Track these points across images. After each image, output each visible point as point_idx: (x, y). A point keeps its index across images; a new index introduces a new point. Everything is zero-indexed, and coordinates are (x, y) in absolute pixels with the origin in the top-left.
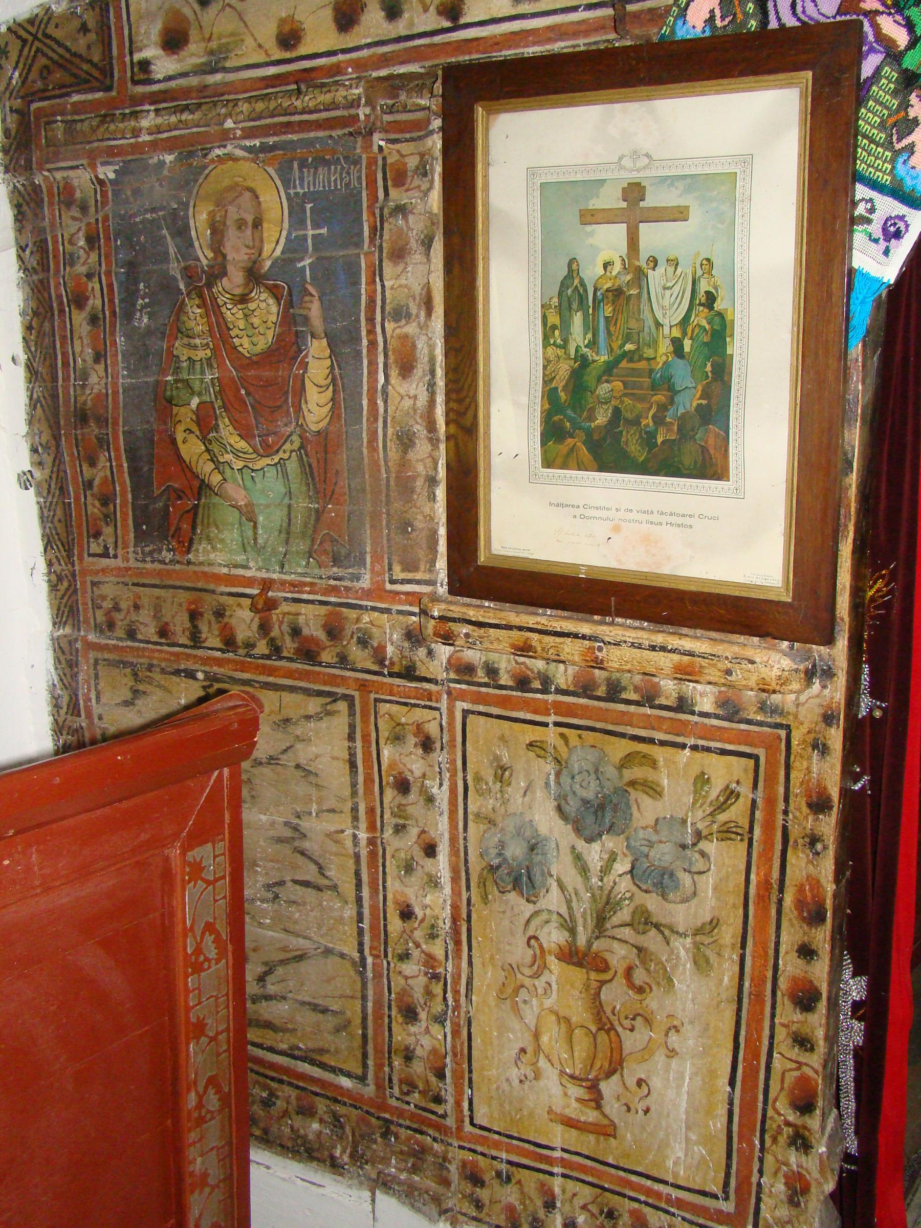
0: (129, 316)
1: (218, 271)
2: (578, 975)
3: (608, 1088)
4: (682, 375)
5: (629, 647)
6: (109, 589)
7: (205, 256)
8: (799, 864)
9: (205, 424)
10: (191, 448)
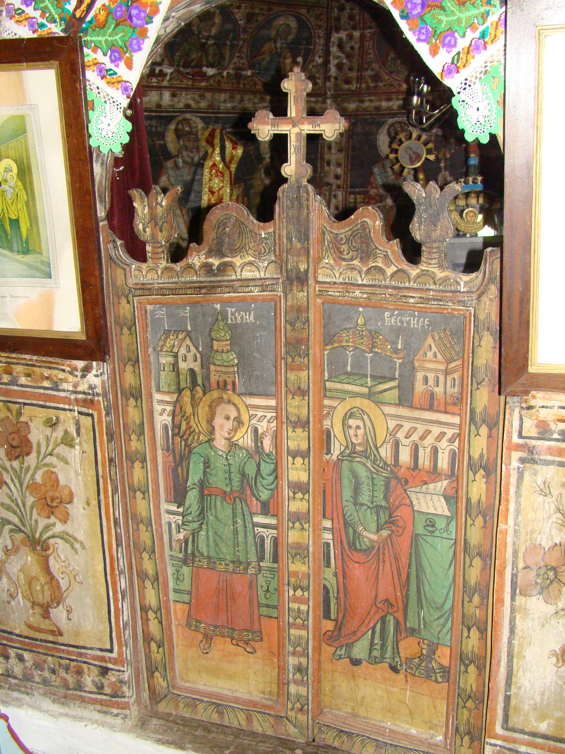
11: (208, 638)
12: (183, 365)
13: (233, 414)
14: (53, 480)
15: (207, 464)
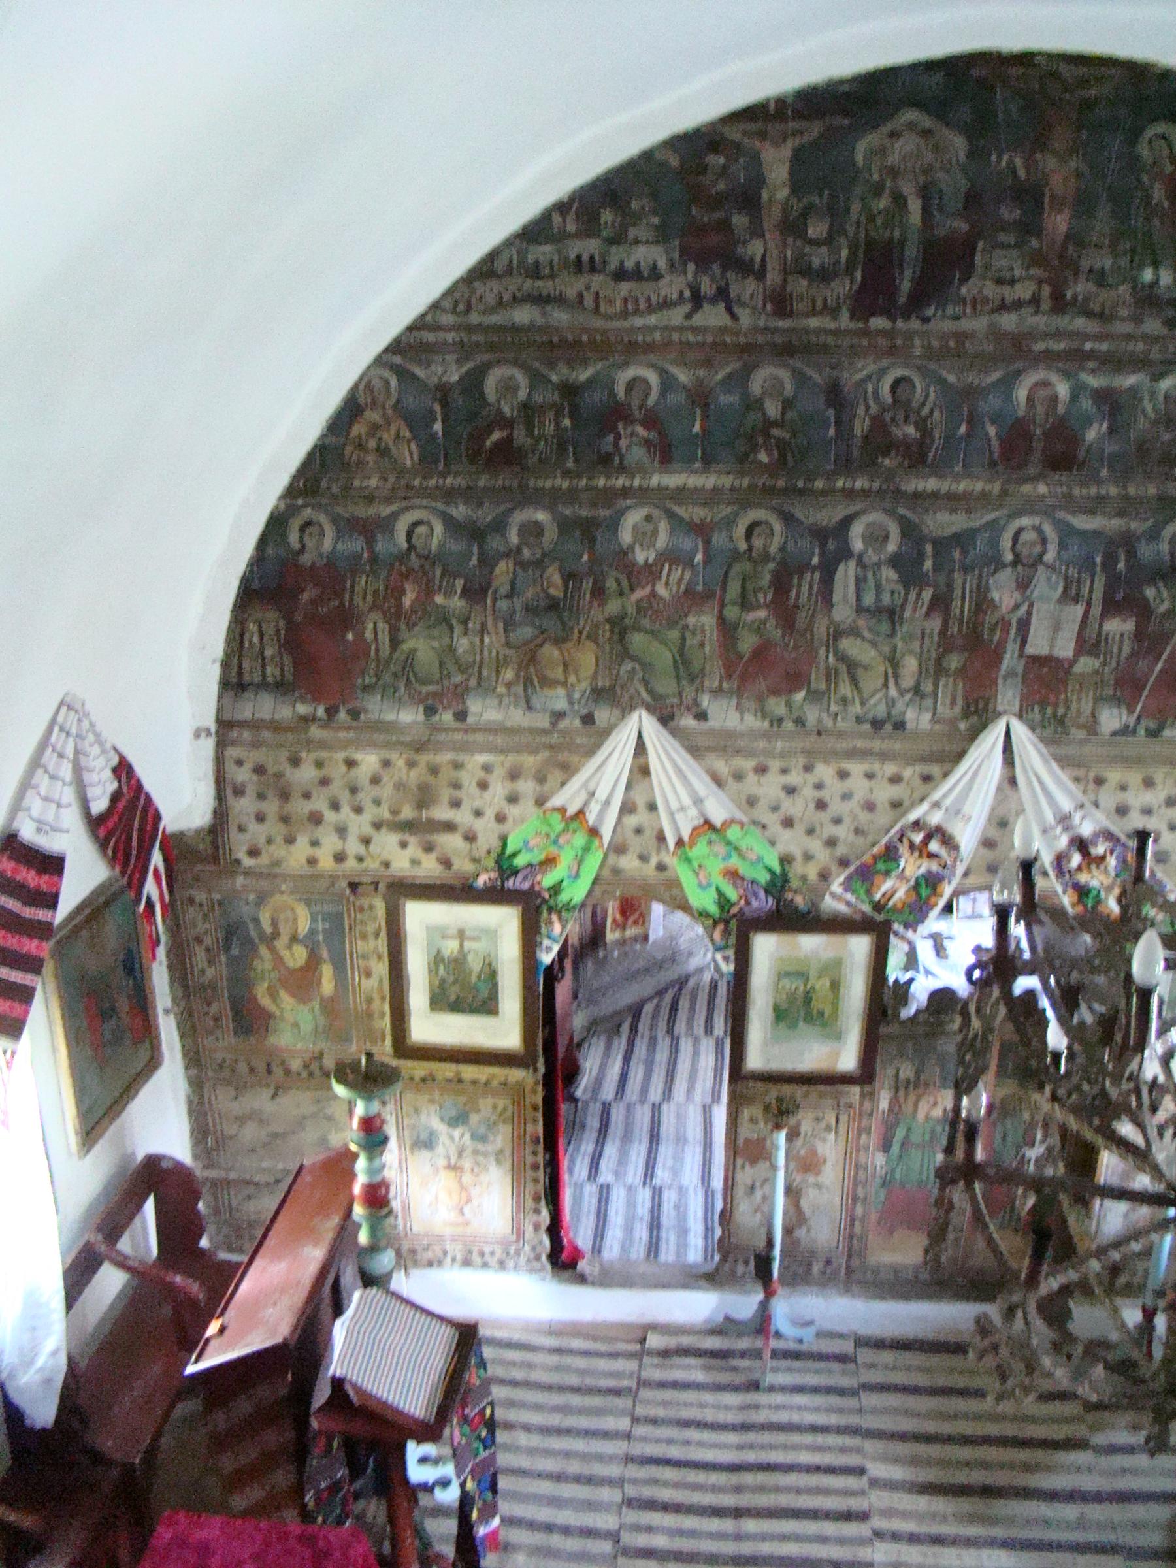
0: (227, 948)
1: (276, 935)
2: (452, 1174)
3: (466, 1210)
4: (481, 985)
5: (469, 1072)
6: (219, 1056)
7: (268, 929)
8: (530, 1128)
9: (272, 993)
10: (265, 1001)
11: (891, 1232)
12: (902, 1075)
13: (932, 1099)
14: (814, 1152)
15: (909, 1130)
